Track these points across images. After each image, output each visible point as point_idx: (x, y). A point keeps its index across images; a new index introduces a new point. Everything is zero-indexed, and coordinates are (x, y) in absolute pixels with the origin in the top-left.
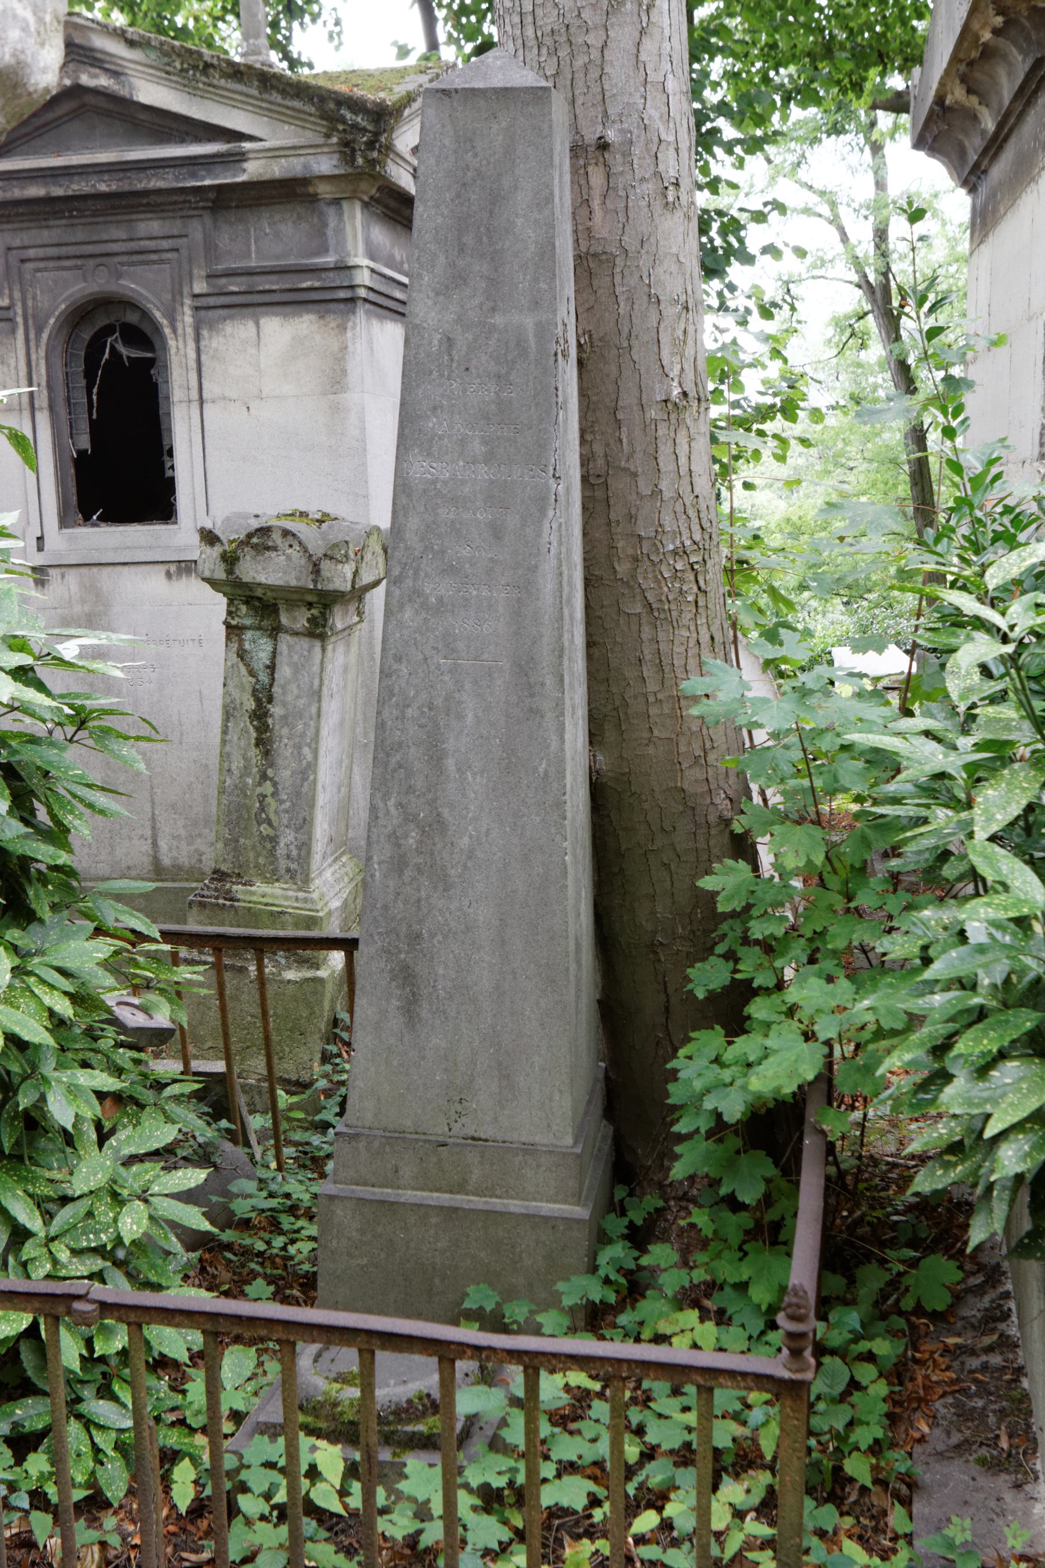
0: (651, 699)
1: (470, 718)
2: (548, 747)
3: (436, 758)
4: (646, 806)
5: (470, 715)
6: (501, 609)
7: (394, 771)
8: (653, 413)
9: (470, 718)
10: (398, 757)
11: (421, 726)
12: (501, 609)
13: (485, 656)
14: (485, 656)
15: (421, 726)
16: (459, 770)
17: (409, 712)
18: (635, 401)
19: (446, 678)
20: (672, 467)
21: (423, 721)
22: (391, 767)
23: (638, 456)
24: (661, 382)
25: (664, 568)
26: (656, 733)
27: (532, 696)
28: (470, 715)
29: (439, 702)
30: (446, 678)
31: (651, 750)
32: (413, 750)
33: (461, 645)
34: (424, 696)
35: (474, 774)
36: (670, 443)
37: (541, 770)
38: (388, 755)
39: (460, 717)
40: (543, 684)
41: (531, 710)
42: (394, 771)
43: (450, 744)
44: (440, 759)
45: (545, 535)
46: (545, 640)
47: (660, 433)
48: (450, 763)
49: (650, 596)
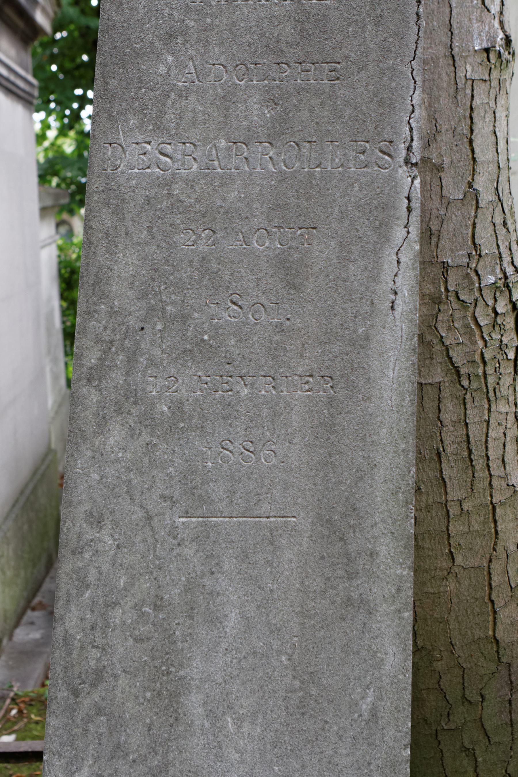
0: (454, 510)
1: (233, 621)
2: (380, 665)
3: (167, 694)
4: (439, 666)
5: (233, 616)
6: (295, 420)
7: (88, 719)
8: (470, 69)
9: (233, 621)
10: (96, 697)
11: (138, 640)
12: (295, 420)
13: (265, 508)
14: (265, 508)
15: (138, 640)
16: (209, 714)
17: (117, 615)
18: (442, 51)
19: (189, 551)
20: (490, 155)
21: (144, 629)
22: (80, 715)
23: (445, 138)
24: (481, 21)
25: (479, 312)
26: (459, 559)
27: (351, 576)
28: (233, 616)
29: (174, 594)
30: (189, 551)
31: (451, 585)
32: (123, 681)
33: (217, 491)
34: (145, 584)
35: (239, 720)
36: (489, 117)
37: (365, 707)
38: (76, 693)
39: (214, 620)
40: (372, 554)
41: (349, 601)
42: (88, 719)
43: (195, 669)
44: (174, 696)
45: (387, 276)
46: (380, 474)
47: (477, 101)
48: (194, 703)
49: (458, 359)
